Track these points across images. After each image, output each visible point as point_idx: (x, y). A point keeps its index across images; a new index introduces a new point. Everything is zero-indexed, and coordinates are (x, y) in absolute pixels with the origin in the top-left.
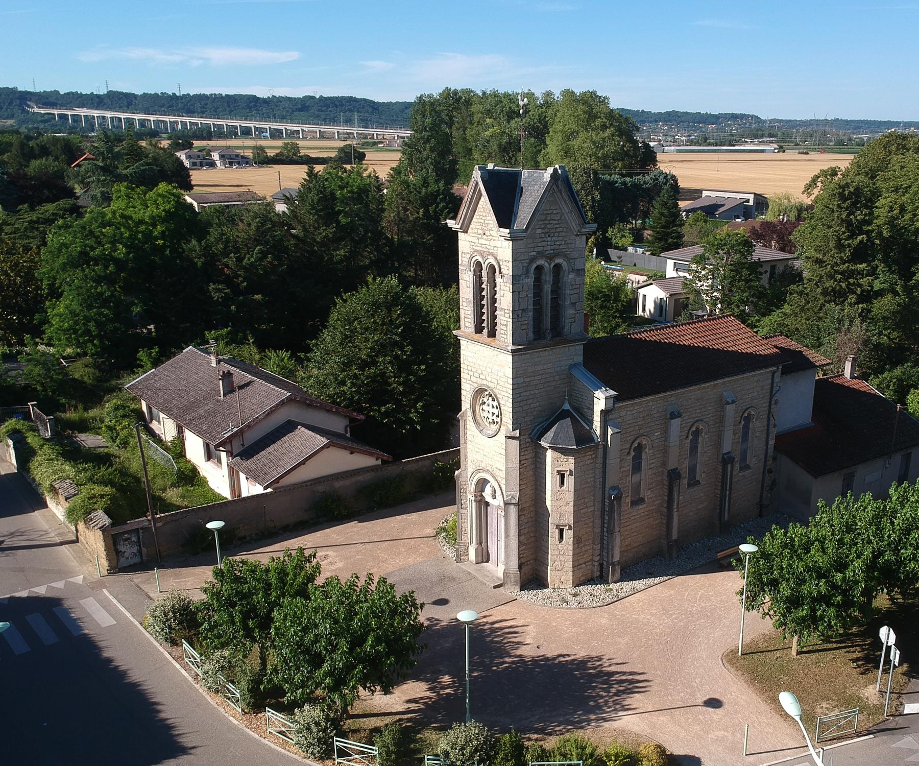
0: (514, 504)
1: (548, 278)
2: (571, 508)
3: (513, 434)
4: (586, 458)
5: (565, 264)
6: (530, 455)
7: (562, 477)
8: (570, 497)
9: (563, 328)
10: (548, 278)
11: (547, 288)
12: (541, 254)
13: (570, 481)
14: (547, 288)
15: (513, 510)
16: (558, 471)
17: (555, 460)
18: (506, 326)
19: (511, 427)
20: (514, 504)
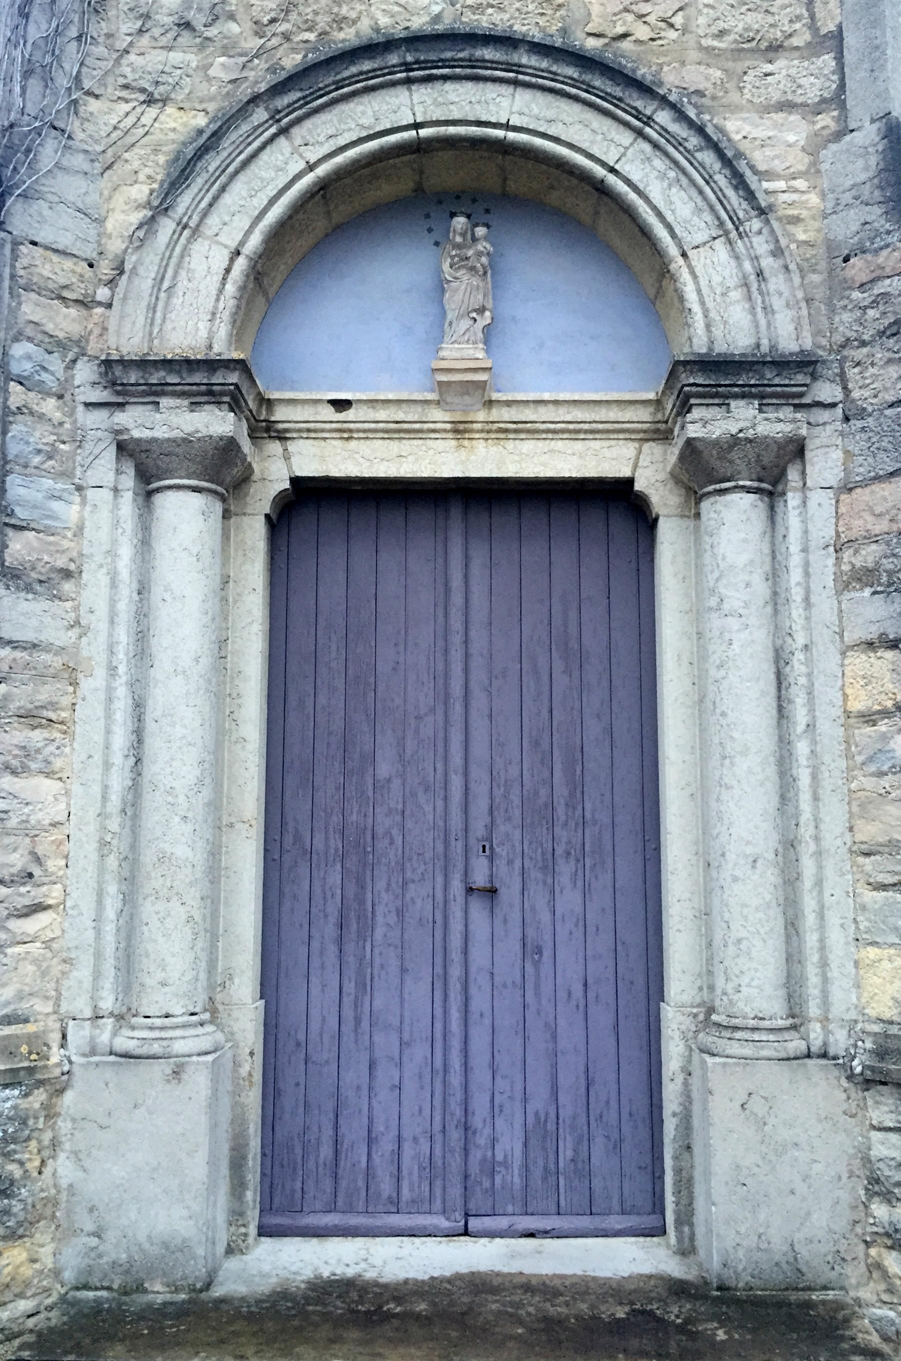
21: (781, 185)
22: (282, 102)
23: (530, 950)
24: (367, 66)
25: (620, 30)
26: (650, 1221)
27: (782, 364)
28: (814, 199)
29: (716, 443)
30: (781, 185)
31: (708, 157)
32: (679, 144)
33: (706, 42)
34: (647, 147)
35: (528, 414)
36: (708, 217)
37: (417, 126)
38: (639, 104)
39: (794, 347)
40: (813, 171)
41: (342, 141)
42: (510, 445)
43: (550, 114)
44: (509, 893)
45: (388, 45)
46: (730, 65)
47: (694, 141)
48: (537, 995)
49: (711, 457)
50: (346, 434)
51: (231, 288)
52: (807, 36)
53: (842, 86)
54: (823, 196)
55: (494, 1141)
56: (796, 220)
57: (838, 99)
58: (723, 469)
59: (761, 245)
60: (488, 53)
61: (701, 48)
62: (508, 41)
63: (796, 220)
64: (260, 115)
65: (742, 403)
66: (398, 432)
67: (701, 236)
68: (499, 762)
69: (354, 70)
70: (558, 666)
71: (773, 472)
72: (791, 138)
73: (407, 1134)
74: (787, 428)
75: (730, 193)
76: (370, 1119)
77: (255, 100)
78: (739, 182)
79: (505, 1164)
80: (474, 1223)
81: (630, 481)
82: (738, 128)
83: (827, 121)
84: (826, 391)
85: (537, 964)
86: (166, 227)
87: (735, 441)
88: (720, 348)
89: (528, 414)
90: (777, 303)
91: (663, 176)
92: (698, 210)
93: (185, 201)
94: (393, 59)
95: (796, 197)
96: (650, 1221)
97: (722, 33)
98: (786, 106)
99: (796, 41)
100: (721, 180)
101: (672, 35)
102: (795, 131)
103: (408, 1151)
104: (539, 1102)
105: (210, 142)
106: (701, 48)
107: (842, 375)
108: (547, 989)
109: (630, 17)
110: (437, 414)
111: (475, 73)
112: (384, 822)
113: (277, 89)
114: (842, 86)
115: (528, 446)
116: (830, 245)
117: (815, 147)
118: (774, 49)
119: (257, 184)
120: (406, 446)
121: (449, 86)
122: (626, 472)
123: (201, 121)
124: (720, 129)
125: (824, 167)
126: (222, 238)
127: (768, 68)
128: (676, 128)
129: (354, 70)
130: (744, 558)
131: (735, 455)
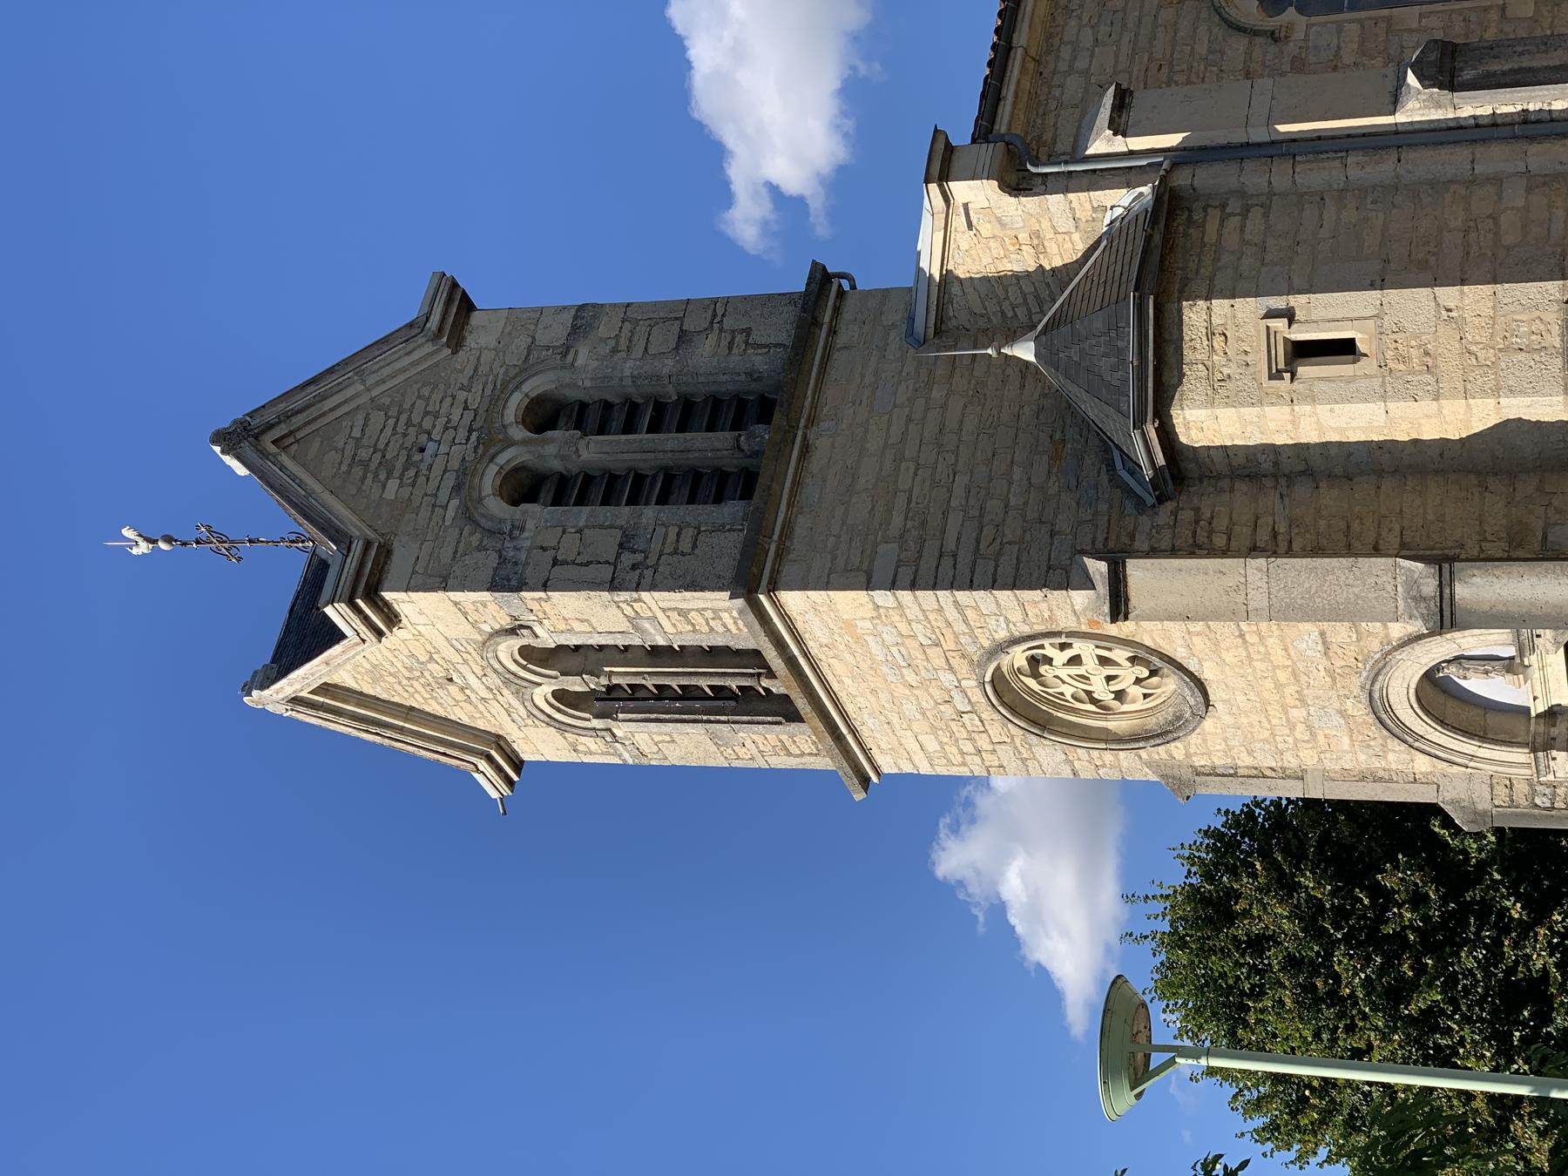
0: (1445, 584)
1: (563, 450)
2: (1473, 300)
3: (1103, 588)
4: (1231, 239)
5: (536, 385)
6: (1239, 504)
7: (1305, 351)
8: (1412, 306)
9: (752, 375)
10: (563, 450)
11: (593, 451)
12: (464, 482)
13: (1324, 314)
14: (593, 451)
15: (1479, 587)
16: (1275, 375)
17: (1219, 390)
18: (683, 613)
19: (1080, 598)
20: (1445, 584)
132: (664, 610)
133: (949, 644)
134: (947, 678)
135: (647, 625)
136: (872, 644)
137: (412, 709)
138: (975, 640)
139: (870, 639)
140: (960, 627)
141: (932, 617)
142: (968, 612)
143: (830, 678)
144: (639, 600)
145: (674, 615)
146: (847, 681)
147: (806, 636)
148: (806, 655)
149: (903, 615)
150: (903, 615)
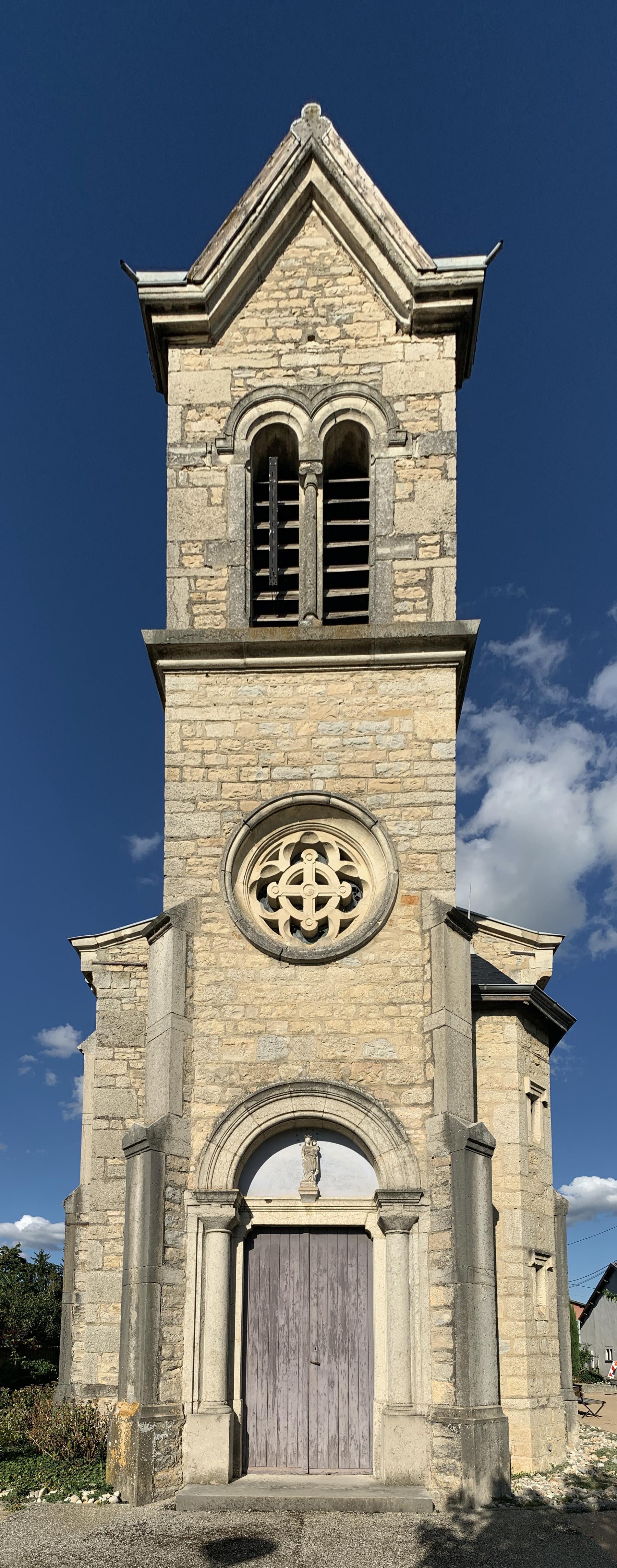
18: (426, 583)
21: (413, 1132)
22: (249, 1105)
23: (331, 1383)
24: (278, 1092)
25: (361, 1078)
26: (370, 1470)
27: (411, 1192)
28: (423, 1137)
29: (389, 1218)
30: (413, 1132)
31: (388, 1123)
32: (379, 1119)
33: (390, 1082)
34: (369, 1119)
35: (330, 1204)
36: (388, 1143)
37: (294, 1112)
38: (366, 1106)
39: (415, 1187)
40: (423, 1127)
41: (269, 1117)
42: (324, 1214)
43: (337, 1108)
44: (324, 1364)
45: (285, 1085)
46: (396, 1090)
47: (384, 1118)
48: (333, 1398)
49: (388, 1223)
50: (270, 1210)
51: (234, 1167)
52: (423, 1080)
53: (433, 1099)
54: (426, 1135)
55: (318, 1445)
56: (417, 1144)
57: (431, 1104)
58: (393, 1226)
59: (405, 1153)
60: (317, 1088)
61: (388, 1085)
62: (324, 1084)
63: (417, 1144)
64: (242, 1109)
65: (398, 1205)
66: (287, 1209)
67: (386, 1150)
68: (320, 1320)
69: (273, 1094)
70: (340, 1288)
71: (408, 1226)
72: (417, 1116)
73: (290, 1443)
74: (412, 1213)
75: (395, 1135)
76: (278, 1438)
77: (241, 1104)
78: (399, 1132)
79: (321, 1452)
80: (311, 1471)
81: (364, 1226)
82: (399, 1112)
83: (428, 1111)
84: (424, 1201)
85: (332, 1387)
86: (213, 1147)
87: (396, 1218)
88: (391, 1187)
89: (330, 1204)
90: (410, 1172)
91: (374, 1129)
92: (385, 1141)
93: (218, 1137)
94: (286, 1090)
95: (418, 1136)
96: (370, 1470)
97: (394, 1079)
98: (415, 1105)
99: (418, 1082)
100: (393, 1131)
101: (378, 1080)
102: (417, 1113)
103: (290, 1447)
104: (333, 1432)
105: (226, 1118)
106: (388, 1085)
107: (431, 1196)
108: (336, 1396)
109: (364, 1074)
110: (300, 1204)
111: (312, 1094)
112: (282, 1340)
113: (248, 1101)
114: (433, 1099)
115: (330, 1214)
116: (429, 1153)
117: (425, 1118)
118: (412, 1085)
119: (242, 1132)
120: (290, 1214)
121: (304, 1098)
122: (362, 1223)
123: (224, 1110)
124: (392, 1114)
125: (427, 1126)
126: (231, 1150)
127: (410, 1091)
128: (378, 1114)
129: (273, 1094)
130: (399, 1255)
131: (396, 1222)
132: (430, 570)
133: (374, 783)
134: (328, 770)
135: (406, 547)
136: (378, 724)
137: (261, 280)
138: (388, 806)
139: (386, 724)
140: (405, 799)
141: (420, 782)
142: (425, 810)
143: (326, 676)
144: (443, 554)
145: (422, 575)
146: (321, 688)
147: (389, 675)
148: (367, 665)
149: (419, 759)
150: (419, 759)
